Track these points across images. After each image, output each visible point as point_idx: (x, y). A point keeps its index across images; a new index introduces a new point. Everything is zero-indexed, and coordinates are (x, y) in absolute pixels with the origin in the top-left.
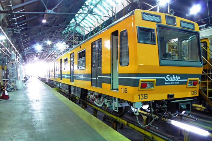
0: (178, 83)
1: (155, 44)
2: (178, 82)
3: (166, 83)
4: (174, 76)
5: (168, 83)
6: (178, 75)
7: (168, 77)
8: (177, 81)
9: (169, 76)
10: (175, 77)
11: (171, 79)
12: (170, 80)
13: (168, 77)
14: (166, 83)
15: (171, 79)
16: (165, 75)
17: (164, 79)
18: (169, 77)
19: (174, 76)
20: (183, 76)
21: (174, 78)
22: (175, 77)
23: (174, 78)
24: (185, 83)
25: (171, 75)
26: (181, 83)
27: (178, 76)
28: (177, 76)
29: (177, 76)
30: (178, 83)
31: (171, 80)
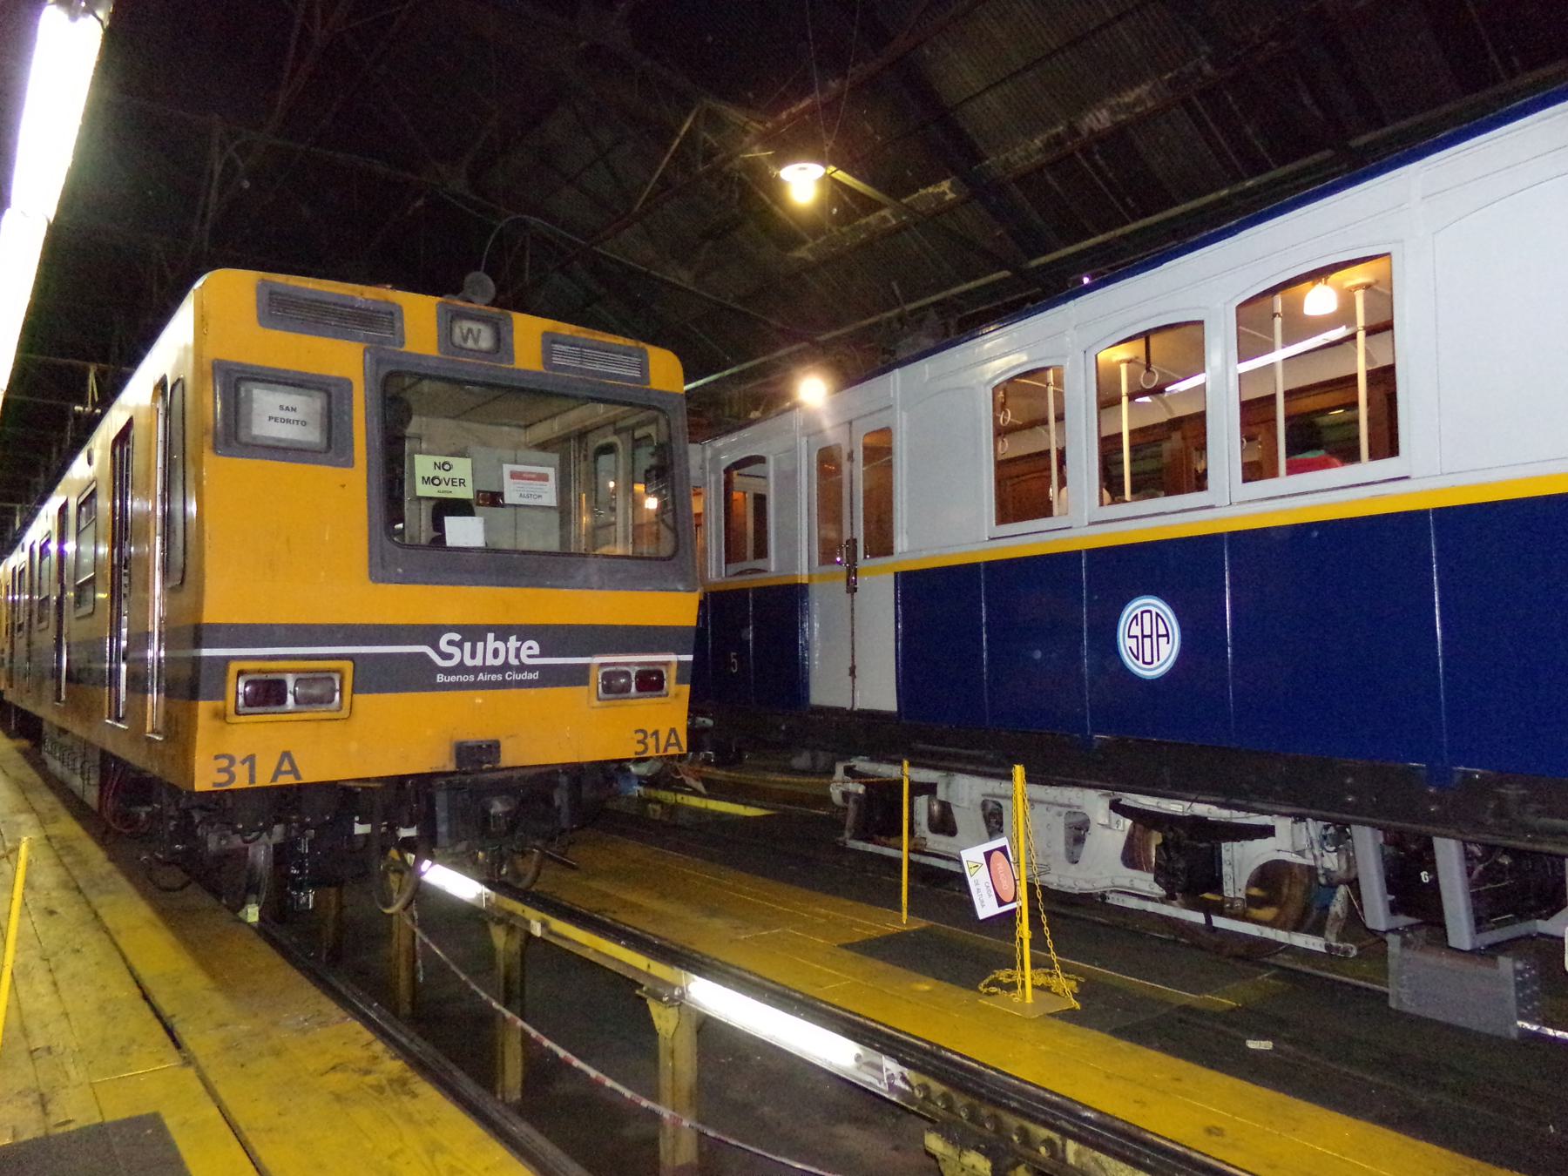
0: (535, 676)
1: (349, 463)
2: (532, 668)
3: (440, 678)
4: (491, 636)
5: (453, 679)
6: (525, 632)
7: (450, 643)
8: (522, 668)
9: (457, 637)
10: (506, 641)
11: (473, 656)
12: (469, 662)
13: (450, 643)
14: (440, 678)
15: (473, 656)
16: (431, 634)
17: (423, 655)
18: (460, 645)
19: (491, 636)
20: (554, 638)
21: (491, 651)
22: (500, 645)
23: (491, 651)
24: (578, 676)
25: (473, 633)
26: (551, 677)
27: (522, 639)
28: (513, 638)
29: (513, 638)
30: (535, 676)
31: (478, 662)
